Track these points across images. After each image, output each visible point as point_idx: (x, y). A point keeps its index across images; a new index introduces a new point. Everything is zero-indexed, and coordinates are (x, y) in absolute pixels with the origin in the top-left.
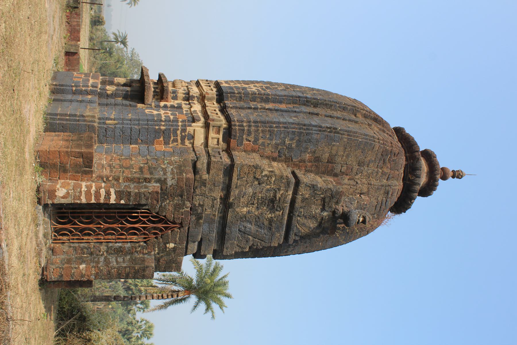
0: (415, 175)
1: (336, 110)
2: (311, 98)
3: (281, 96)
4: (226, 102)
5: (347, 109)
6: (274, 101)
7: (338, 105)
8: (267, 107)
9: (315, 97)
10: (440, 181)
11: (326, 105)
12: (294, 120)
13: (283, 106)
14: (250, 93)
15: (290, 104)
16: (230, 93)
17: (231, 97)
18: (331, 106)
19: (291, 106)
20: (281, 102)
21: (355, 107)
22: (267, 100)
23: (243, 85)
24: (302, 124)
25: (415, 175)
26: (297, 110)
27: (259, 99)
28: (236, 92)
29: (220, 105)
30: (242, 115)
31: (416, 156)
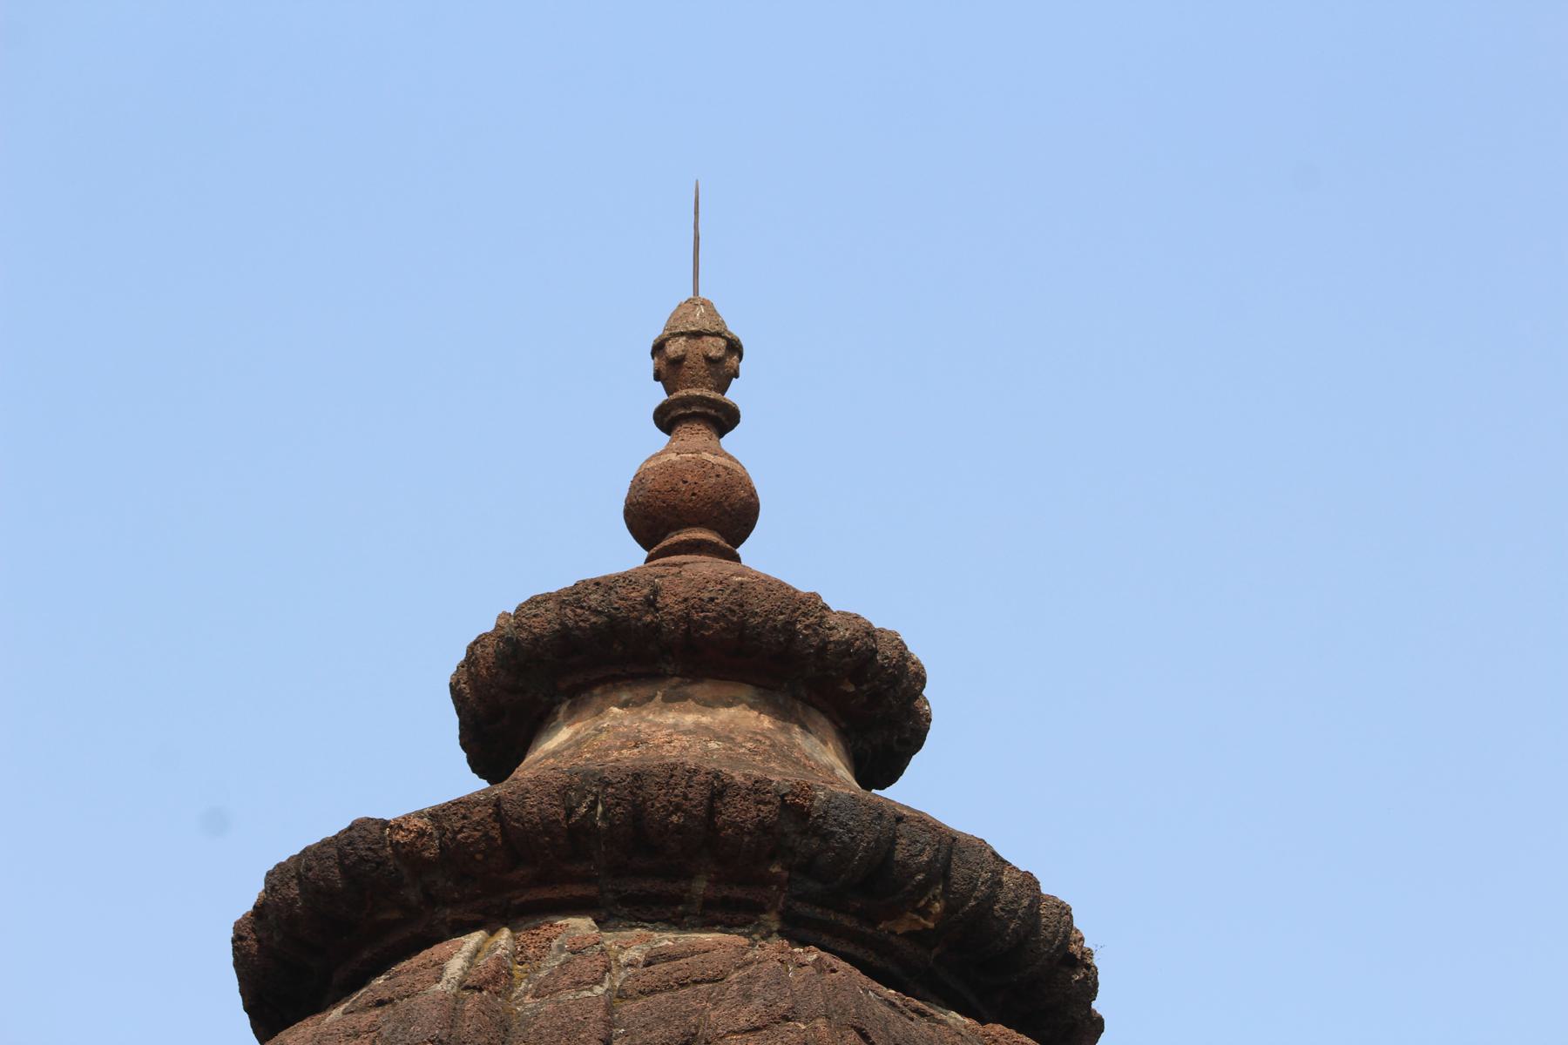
0: (924, 887)
10: (761, 554)
25: (924, 887)
31: (763, 827)
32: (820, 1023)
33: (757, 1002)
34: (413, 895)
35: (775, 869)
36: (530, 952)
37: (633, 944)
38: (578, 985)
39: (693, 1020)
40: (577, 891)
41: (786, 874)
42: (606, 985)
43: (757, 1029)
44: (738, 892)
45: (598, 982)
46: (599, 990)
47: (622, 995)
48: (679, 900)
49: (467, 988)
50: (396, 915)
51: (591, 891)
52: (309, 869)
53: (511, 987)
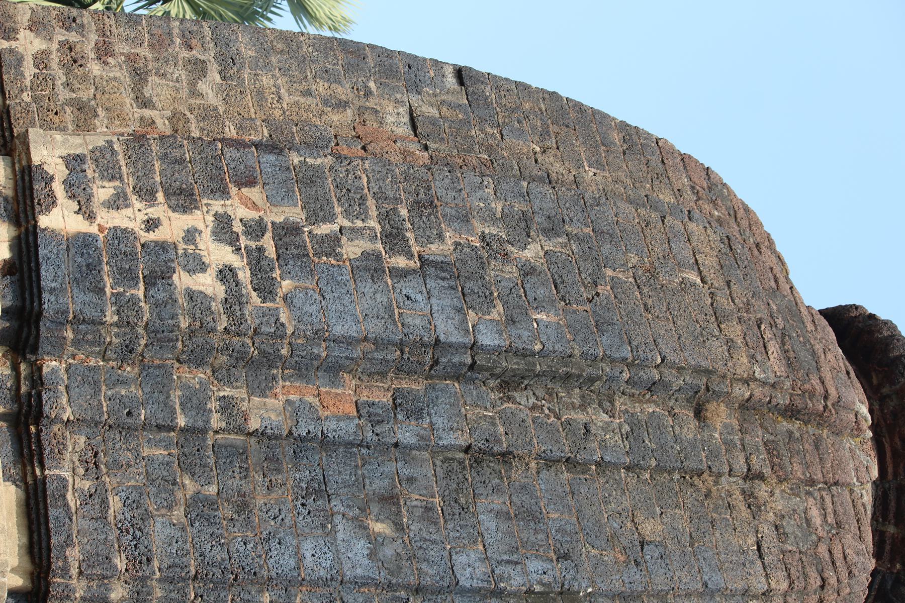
1: (607, 402)
2: (498, 350)
3: (349, 342)
4: (50, 365)
5: (666, 386)
6: (303, 368)
7: (626, 375)
8: (254, 424)
9: (521, 336)
11: (568, 376)
12: (376, 542)
13: (337, 405)
14: (184, 323)
15: (383, 375)
16: (78, 321)
17: (76, 343)
18: (592, 380)
19: (379, 395)
20: (333, 370)
21: (708, 372)
22: (259, 362)
23: (159, 211)
24: (407, 587)
26: (406, 433)
27: (223, 359)
28: (111, 317)
29: (15, 368)
30: (115, 503)
32: (848, 590)
33: (856, 559)
34: (885, 390)
35: (898, 566)
36: (865, 446)
37: (867, 497)
38: (857, 470)
39: (847, 526)
40: (890, 470)
41: (895, 571)
42: (857, 484)
43: (845, 558)
44: (888, 548)
45: (858, 479)
46: (855, 479)
47: (851, 491)
48: (885, 519)
49: (856, 415)
50: (875, 381)
51: (890, 477)
52: (898, 340)
53: (852, 436)
